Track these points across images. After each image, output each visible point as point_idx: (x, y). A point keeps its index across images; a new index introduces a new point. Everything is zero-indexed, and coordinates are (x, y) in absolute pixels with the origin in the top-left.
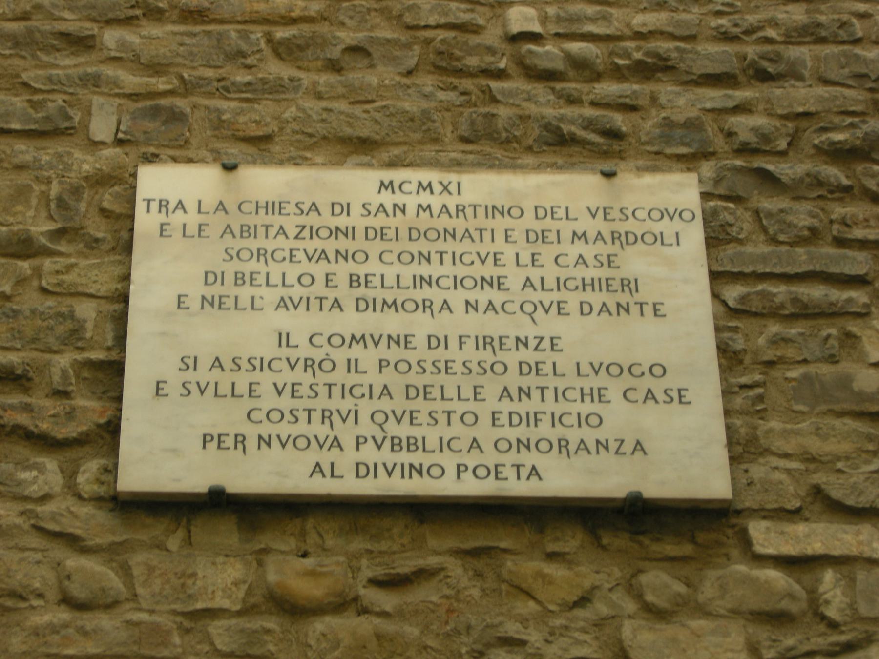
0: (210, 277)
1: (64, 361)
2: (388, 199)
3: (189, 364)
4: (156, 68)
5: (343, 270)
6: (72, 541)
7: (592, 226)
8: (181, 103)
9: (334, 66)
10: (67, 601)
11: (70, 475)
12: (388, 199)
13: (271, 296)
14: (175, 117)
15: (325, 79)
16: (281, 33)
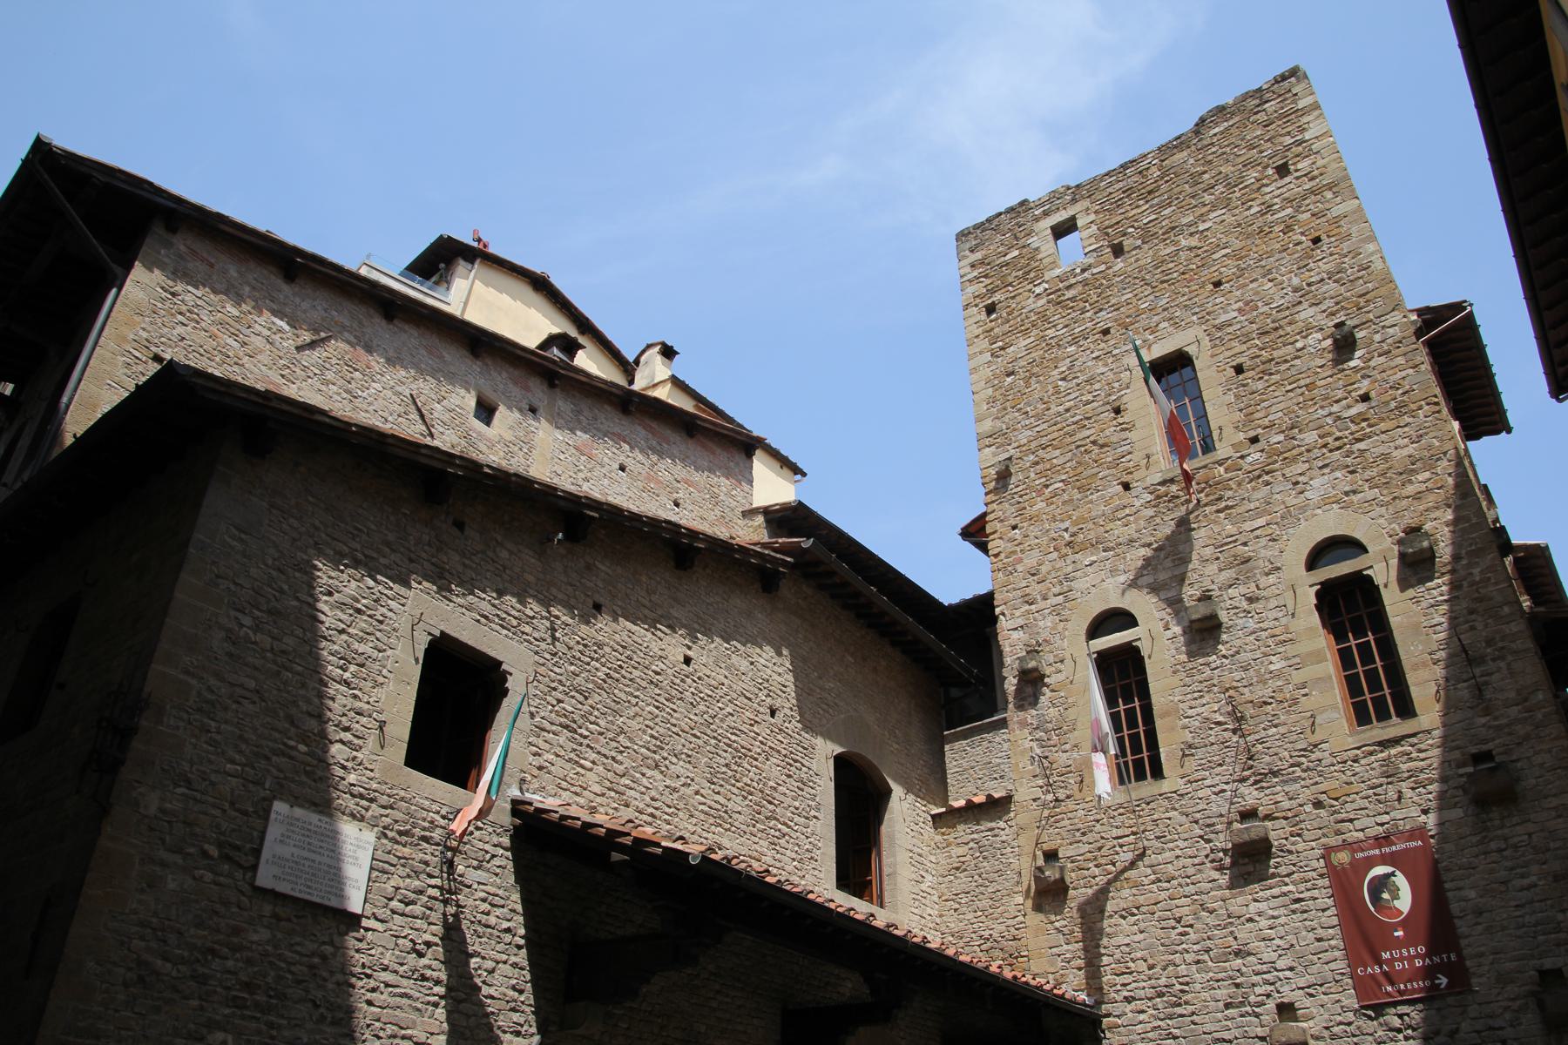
0: (283, 835)
1: (248, 846)
2: (319, 824)
3: (274, 856)
4: (280, 771)
5: (307, 839)
6: (242, 892)
7: (353, 841)
8: (284, 782)
9: (315, 781)
10: (239, 907)
11: (244, 875)
12: (319, 824)
13: (292, 843)
14: (282, 786)
15: (313, 783)
16: (308, 768)
